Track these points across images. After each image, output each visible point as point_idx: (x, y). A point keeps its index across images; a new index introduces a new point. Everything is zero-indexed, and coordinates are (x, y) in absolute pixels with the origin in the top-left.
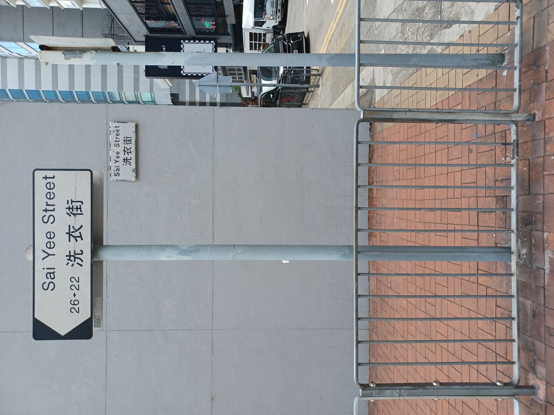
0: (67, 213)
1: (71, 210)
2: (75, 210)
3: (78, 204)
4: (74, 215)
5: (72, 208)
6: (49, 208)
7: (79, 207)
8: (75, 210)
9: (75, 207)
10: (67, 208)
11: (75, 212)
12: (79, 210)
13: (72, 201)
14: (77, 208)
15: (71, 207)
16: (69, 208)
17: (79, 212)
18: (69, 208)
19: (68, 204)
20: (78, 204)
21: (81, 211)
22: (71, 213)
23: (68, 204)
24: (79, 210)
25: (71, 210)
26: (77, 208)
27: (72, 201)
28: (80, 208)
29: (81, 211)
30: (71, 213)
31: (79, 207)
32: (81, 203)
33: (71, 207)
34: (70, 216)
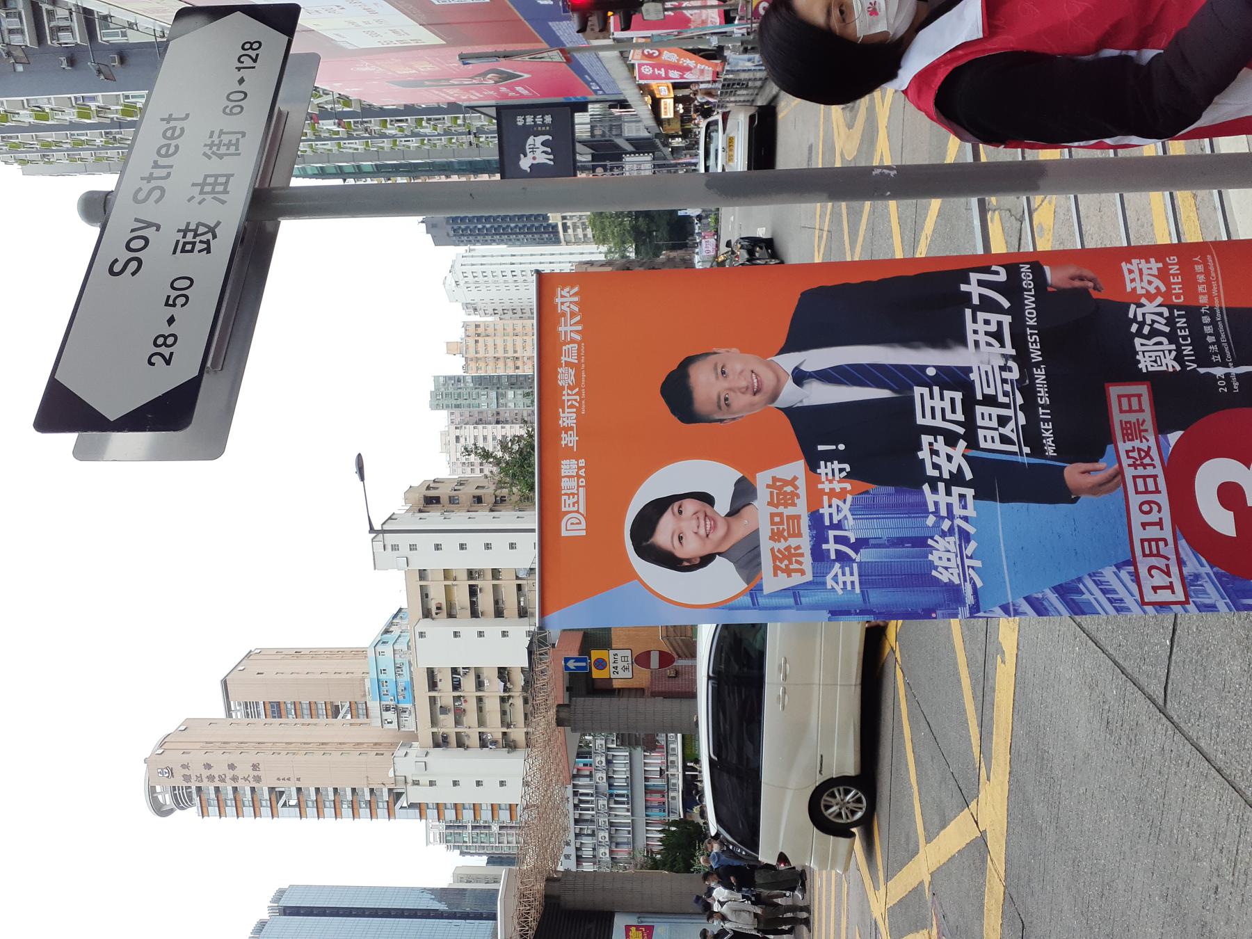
0: (205, 154)
1: (215, 148)
2: (223, 150)
3: (234, 138)
4: (221, 157)
11: (223, 150)
18: (211, 146)
19: (211, 137)
20: (234, 138)
21: (237, 149)
22: (213, 153)
23: (211, 137)
24: (232, 149)
25: (215, 148)
26: (229, 145)
28: (237, 145)
29: (237, 149)
34: (209, 158)
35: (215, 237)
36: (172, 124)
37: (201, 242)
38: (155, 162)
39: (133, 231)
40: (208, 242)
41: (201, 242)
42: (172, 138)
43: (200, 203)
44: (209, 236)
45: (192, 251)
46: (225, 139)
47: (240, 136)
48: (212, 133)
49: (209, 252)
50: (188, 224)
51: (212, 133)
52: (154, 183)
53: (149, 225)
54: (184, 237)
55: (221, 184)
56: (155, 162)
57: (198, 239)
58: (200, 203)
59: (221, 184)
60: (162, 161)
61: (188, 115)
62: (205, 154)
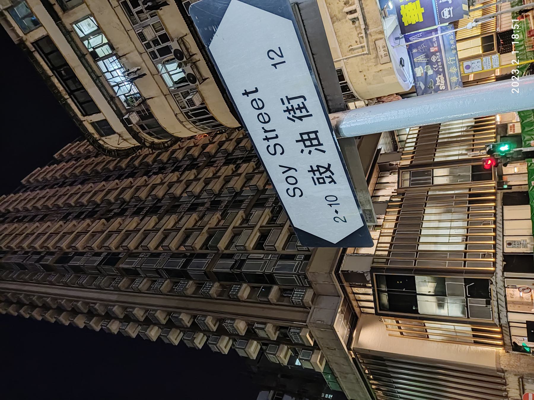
0: (289, 118)
1: (292, 112)
4: (300, 118)
5: (293, 109)
7: (301, 106)
8: (298, 112)
9: (296, 106)
11: (298, 113)
12: (304, 110)
13: (289, 100)
14: (299, 108)
15: (290, 108)
16: (288, 110)
17: (304, 113)
18: (288, 110)
19: (284, 104)
21: (308, 112)
22: (293, 116)
23: (284, 104)
24: (304, 110)
25: (292, 112)
26: (299, 108)
27: (289, 100)
28: (304, 107)
29: (308, 112)
30: (293, 116)
31: (301, 106)
33: (290, 108)
34: (294, 121)
35: (333, 174)
36: (252, 96)
37: (326, 177)
38: (263, 128)
39: (283, 173)
40: (330, 177)
41: (326, 177)
42: (259, 109)
43: (310, 152)
44: (328, 174)
45: (324, 183)
46: (295, 103)
47: (302, 100)
48: (282, 99)
49: (335, 183)
50: (311, 167)
51: (282, 99)
52: (272, 142)
53: (290, 169)
54: (315, 175)
55: (314, 139)
56: (263, 128)
57: (323, 176)
58: (310, 152)
59: (314, 139)
60: (268, 127)
61: (256, 88)
62: (289, 118)
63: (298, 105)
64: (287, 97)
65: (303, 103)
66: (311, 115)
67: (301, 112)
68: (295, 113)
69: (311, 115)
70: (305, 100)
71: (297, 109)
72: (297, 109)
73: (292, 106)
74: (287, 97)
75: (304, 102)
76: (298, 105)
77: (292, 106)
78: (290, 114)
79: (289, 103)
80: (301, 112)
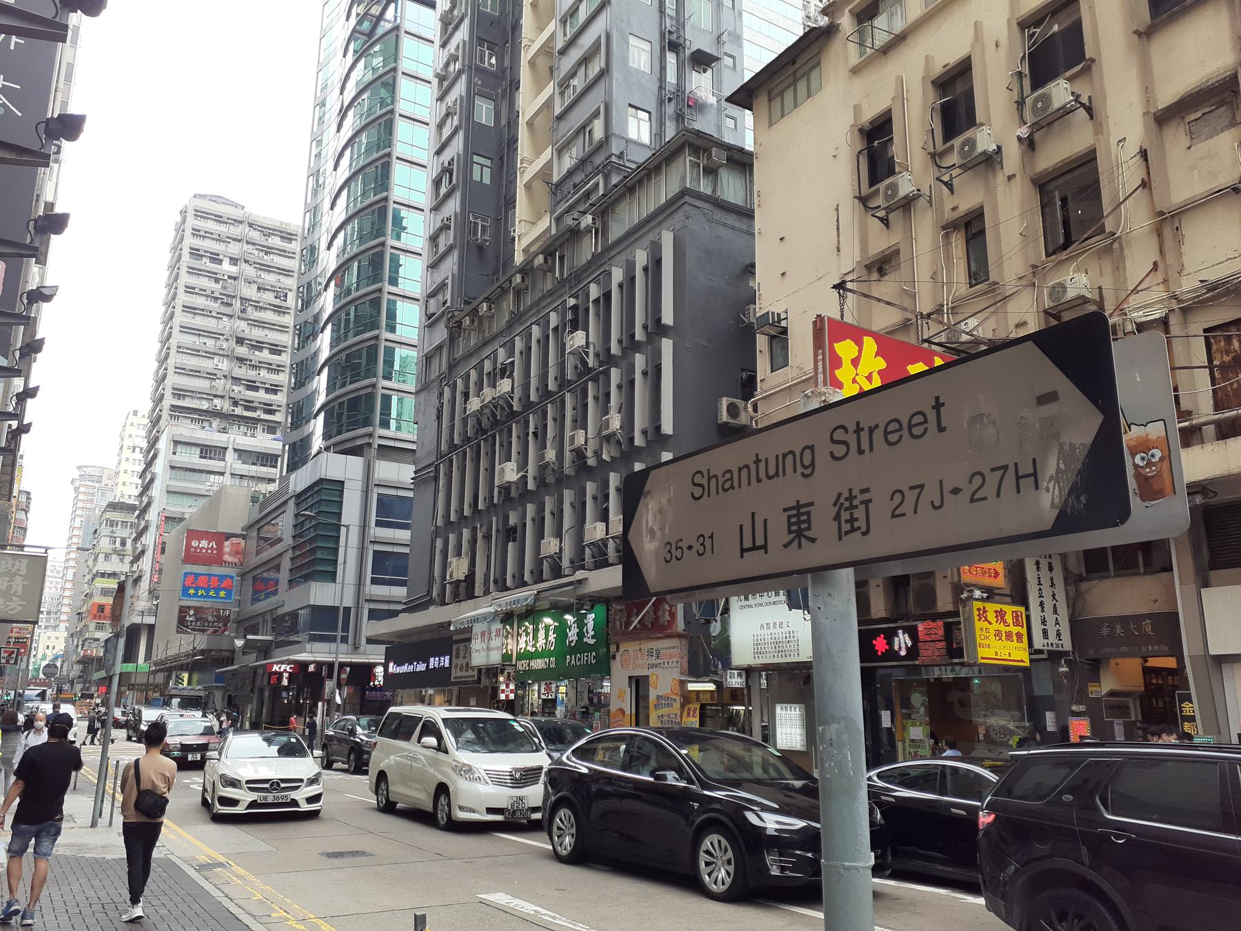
3: (861, 523)
4: (837, 517)
6: (864, 435)
7: (856, 525)
10: (850, 490)
11: (845, 515)
13: (867, 503)
14: (852, 520)
16: (851, 498)
18: (851, 498)
20: (861, 523)
21: (847, 533)
26: (852, 520)
28: (853, 530)
29: (847, 533)
31: (856, 525)
32: (864, 529)
33: (855, 502)
34: (835, 505)
46: (859, 513)
63: (857, 519)
64: (870, 501)
65: (859, 528)
66: (840, 539)
67: (846, 521)
68: (846, 509)
69: (840, 539)
70: (864, 534)
71: (852, 514)
72: (852, 514)
73: (856, 507)
74: (870, 501)
75: (858, 534)
76: (857, 519)
77: (856, 507)
78: (846, 499)
79: (862, 503)
80: (846, 521)
